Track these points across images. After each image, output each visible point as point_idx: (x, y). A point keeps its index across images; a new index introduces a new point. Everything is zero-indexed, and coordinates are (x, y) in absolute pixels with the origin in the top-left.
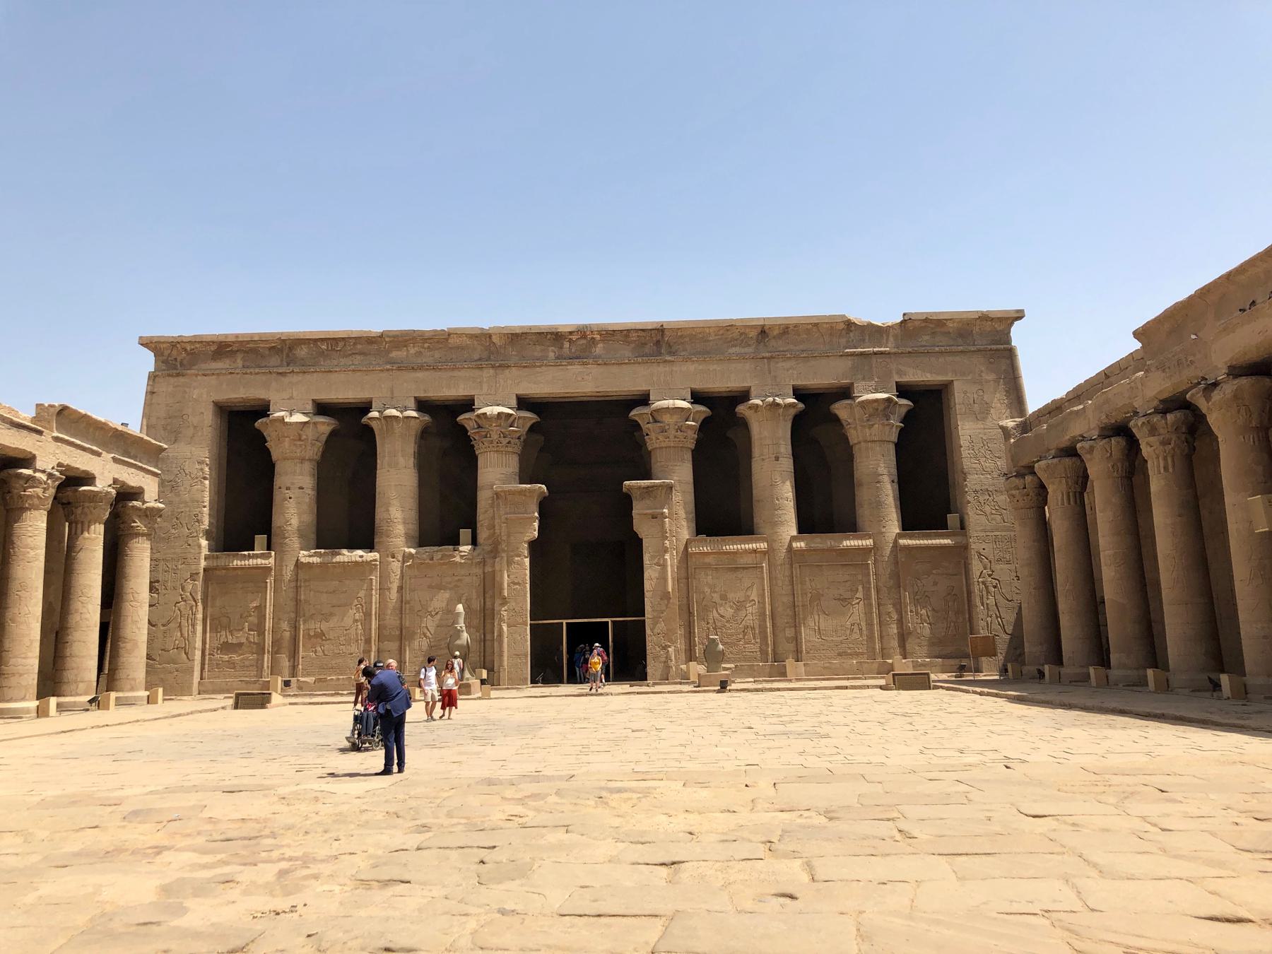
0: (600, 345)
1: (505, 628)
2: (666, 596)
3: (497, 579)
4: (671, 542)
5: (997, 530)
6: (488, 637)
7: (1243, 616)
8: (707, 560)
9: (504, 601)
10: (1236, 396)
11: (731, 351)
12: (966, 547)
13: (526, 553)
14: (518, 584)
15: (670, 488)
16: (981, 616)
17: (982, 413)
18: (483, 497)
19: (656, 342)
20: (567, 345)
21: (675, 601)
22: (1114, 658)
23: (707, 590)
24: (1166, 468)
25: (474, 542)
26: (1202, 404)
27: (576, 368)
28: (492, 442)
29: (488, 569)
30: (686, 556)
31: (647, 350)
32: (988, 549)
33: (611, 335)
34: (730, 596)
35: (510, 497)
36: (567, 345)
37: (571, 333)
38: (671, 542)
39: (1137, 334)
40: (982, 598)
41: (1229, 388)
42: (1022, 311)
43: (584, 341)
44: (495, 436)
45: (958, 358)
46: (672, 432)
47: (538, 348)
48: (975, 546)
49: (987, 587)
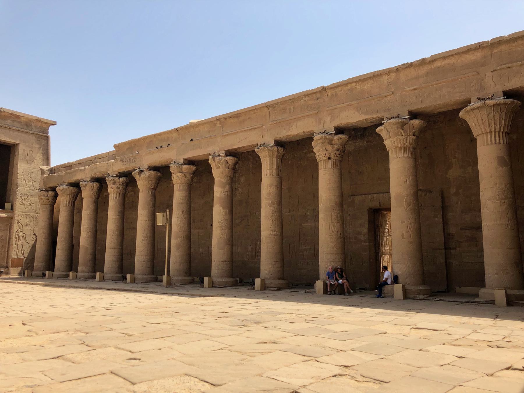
5: (28, 212)
7: (137, 253)
10: (149, 177)
12: (12, 218)
16: (14, 249)
17: (30, 161)
22: (80, 269)
24: (116, 198)
26: (137, 177)
32: (23, 220)
39: (115, 146)
40: (16, 241)
41: (147, 173)
42: (56, 122)
45: (23, 135)
48: (17, 218)
49: (19, 237)
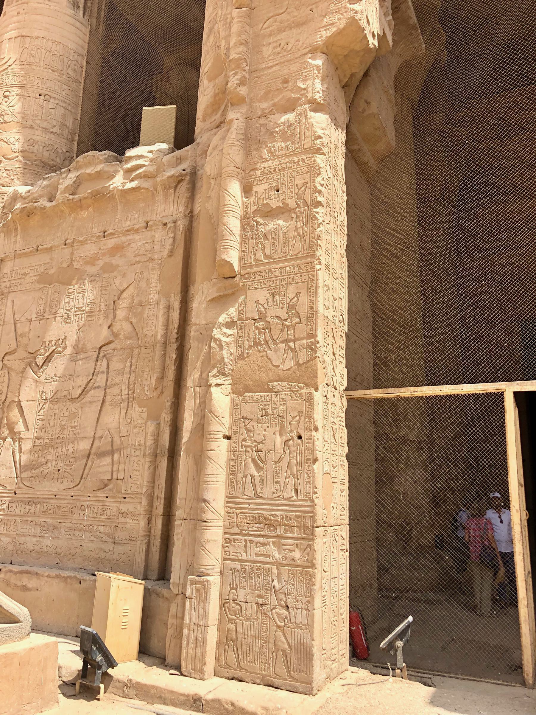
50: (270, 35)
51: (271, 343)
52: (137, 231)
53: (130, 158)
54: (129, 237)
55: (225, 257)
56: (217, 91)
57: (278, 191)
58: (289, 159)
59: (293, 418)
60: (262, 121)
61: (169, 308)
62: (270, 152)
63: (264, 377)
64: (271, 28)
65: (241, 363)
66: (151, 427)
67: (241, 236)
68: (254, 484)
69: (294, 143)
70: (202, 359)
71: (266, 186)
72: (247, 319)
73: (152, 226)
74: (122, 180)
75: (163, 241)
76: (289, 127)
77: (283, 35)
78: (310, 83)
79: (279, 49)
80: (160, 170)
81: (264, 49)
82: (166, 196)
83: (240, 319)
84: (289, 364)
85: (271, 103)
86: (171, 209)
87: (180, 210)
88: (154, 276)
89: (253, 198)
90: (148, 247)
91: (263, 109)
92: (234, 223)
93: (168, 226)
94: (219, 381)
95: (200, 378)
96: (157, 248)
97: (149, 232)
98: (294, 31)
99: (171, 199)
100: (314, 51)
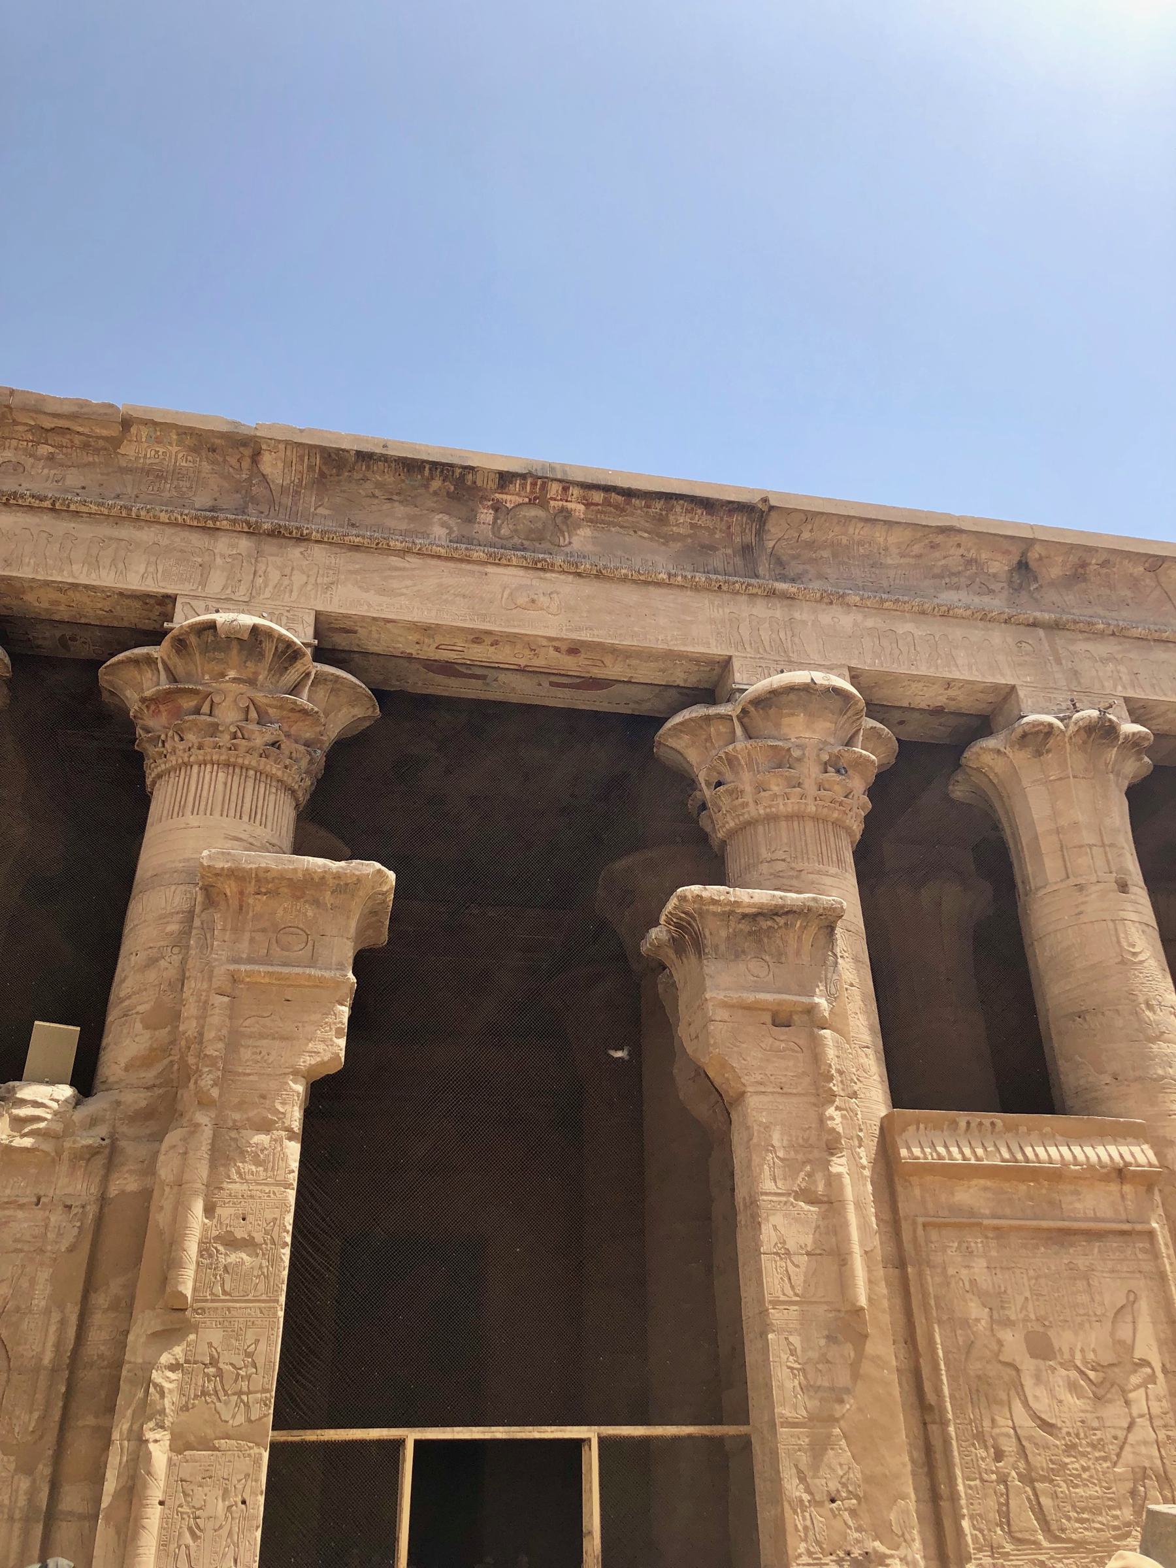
0: (585, 532)
1: (159, 1453)
2: (848, 1326)
3: (160, 1218)
4: (849, 1114)
6: (72, 1499)
8: (967, 1195)
9: (177, 1321)
11: (949, 597)
13: (295, 1117)
14: (248, 1244)
15: (828, 922)
18: (151, 916)
19: (740, 538)
20: (486, 515)
21: (883, 1348)
23: (975, 1310)
25: (84, 1079)
27: (508, 578)
28: (214, 730)
29: (126, 1182)
30: (889, 1170)
31: (717, 561)
33: (618, 500)
34: (1063, 1340)
35: (256, 904)
36: (486, 515)
37: (505, 479)
38: (849, 1114)
43: (534, 512)
44: (228, 715)
46: (811, 772)
47: (400, 510)
50: (250, 1037)
51: (221, 1393)
52: (21, 1207)
53: (23, 1102)
54: (7, 1213)
55: (181, 1288)
56: (155, 1046)
57: (244, 1219)
58: (260, 1188)
59: (239, 1481)
60: (233, 1134)
61: (63, 1322)
62: (239, 1173)
63: (209, 1432)
64: (252, 1029)
65: (184, 1416)
66: (24, 1484)
67: (198, 1263)
68: (188, 1556)
69: (266, 1170)
70: (134, 1406)
71: (232, 1211)
72: (195, 1363)
73: (44, 1203)
74: (9, 1132)
75: (63, 1231)
76: (262, 1151)
77: (264, 1042)
78: (288, 1108)
79: (259, 1057)
80: (68, 1130)
81: (242, 1050)
82: (73, 1168)
83: (187, 1361)
84: (240, 1419)
85: (245, 1116)
86: (78, 1187)
87: (92, 1191)
88: (44, 1275)
89: (215, 1221)
90: (37, 1231)
91: (235, 1121)
92: (192, 1248)
93: (74, 1211)
94: (158, 1437)
95: (130, 1430)
96: (51, 1236)
97: (42, 1212)
98: (277, 1043)
99: (80, 1173)
100: (296, 1073)
